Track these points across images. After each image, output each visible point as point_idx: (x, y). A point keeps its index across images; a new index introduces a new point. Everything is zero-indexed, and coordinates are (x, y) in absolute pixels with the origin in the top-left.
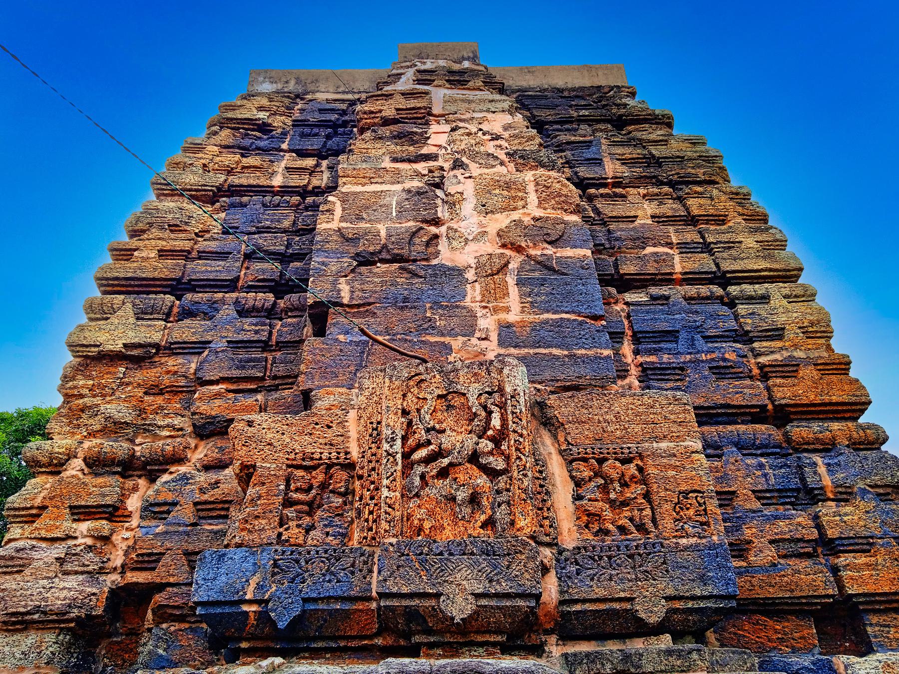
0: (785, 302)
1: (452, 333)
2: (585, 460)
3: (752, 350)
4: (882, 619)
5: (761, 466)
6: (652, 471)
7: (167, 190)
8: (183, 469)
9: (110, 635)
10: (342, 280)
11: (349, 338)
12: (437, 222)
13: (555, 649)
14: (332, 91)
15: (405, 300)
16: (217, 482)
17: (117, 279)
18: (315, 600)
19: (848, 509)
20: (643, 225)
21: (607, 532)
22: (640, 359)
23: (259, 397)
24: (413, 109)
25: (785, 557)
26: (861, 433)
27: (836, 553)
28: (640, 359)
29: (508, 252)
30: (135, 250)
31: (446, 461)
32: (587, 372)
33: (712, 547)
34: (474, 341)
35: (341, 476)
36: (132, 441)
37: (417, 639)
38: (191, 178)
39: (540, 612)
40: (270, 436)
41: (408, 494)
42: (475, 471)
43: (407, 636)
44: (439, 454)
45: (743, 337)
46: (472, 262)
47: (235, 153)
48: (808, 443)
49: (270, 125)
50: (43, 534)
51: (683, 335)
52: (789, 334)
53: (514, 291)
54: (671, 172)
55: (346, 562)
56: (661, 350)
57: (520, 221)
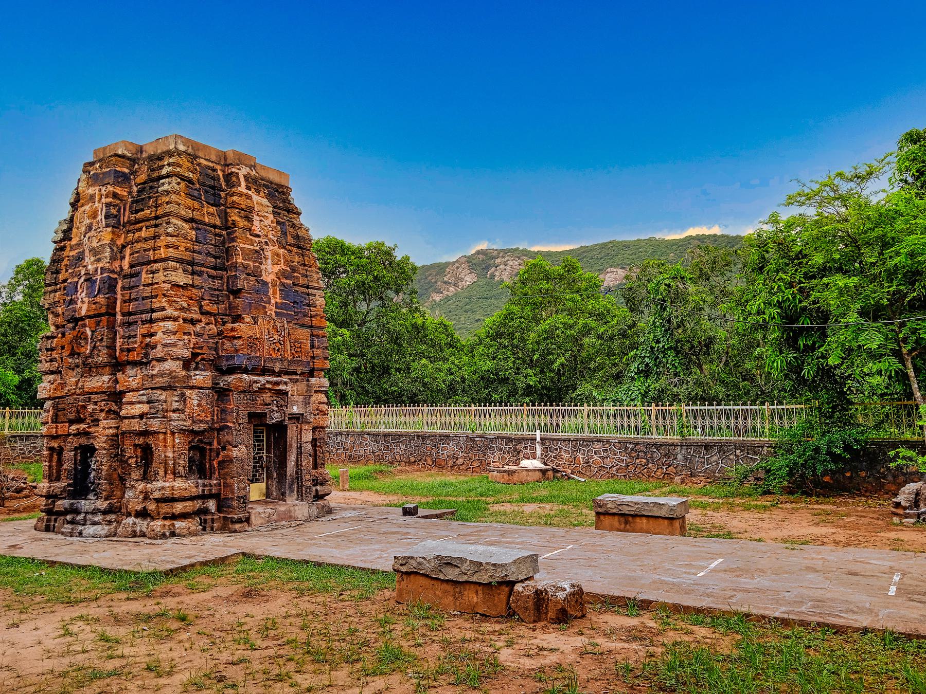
45: (309, 305)
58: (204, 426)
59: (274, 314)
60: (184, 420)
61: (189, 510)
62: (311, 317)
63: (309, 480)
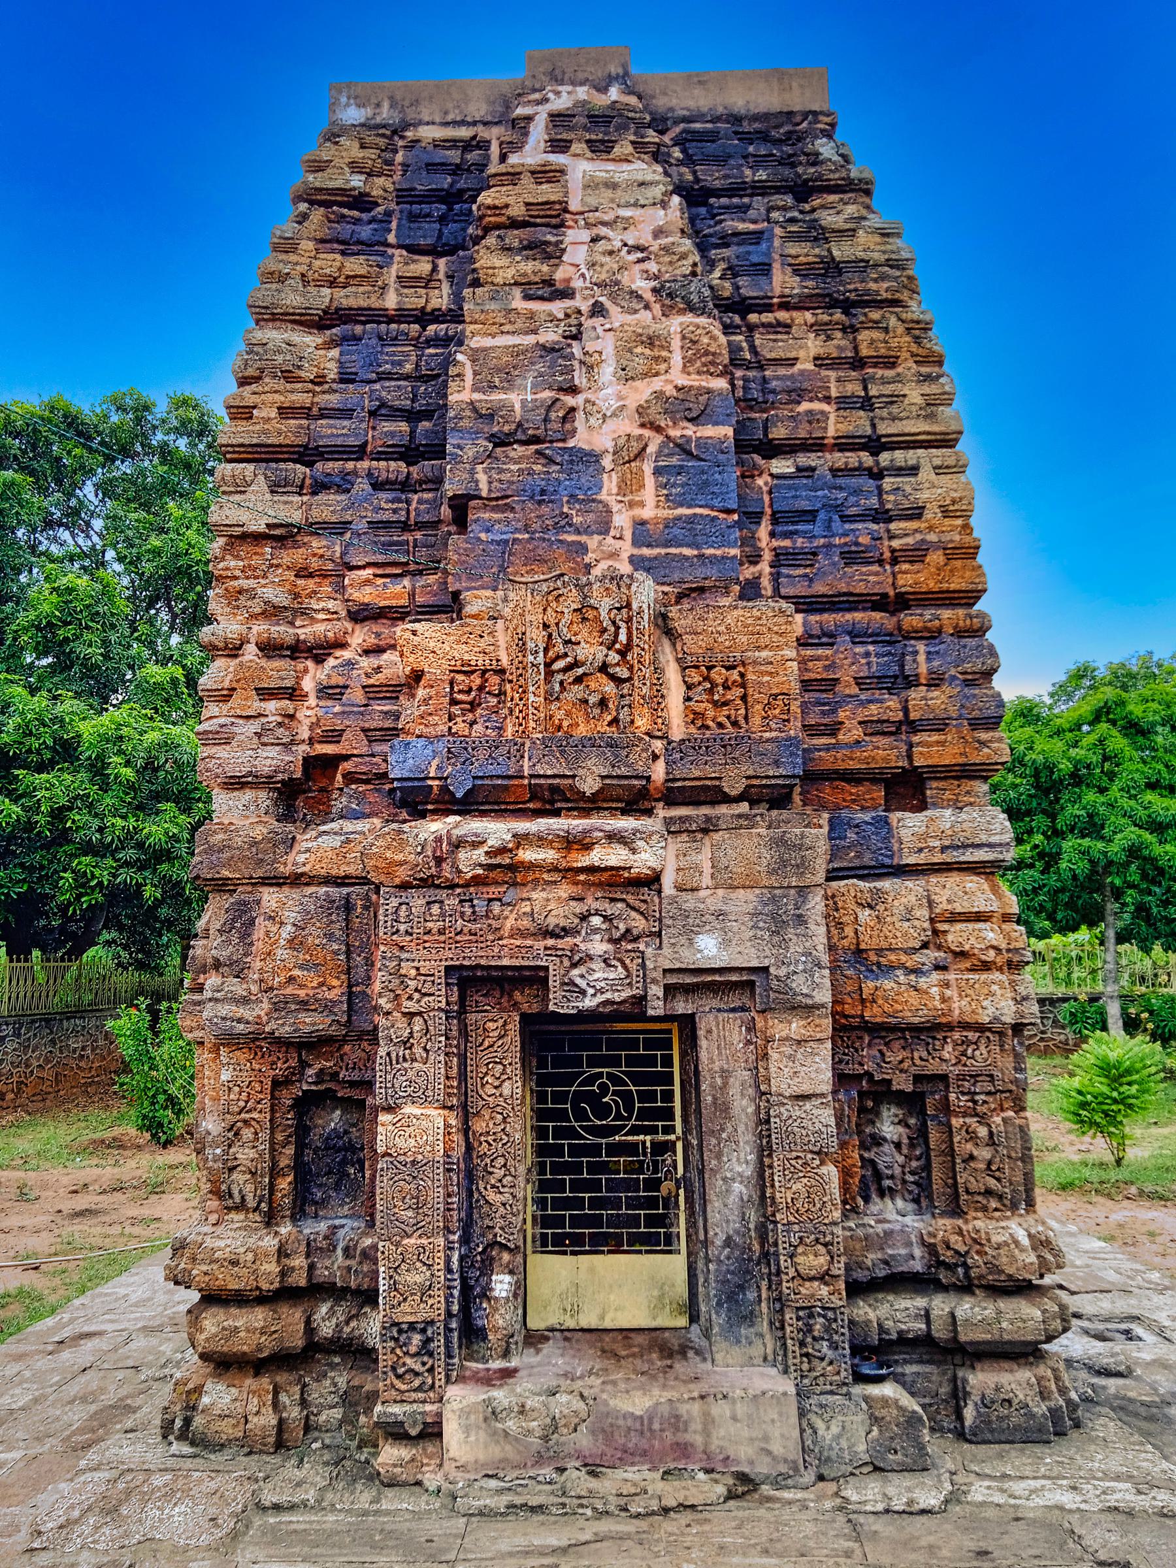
0: (933, 476)
1: (587, 531)
2: (696, 667)
3: (888, 531)
4: (941, 784)
5: (867, 654)
6: (750, 677)
7: (268, 316)
8: (347, 654)
9: (305, 792)
10: (479, 468)
11: (491, 537)
12: (573, 390)
13: (662, 812)
14: (438, 120)
15: (543, 492)
16: (379, 667)
17: (242, 445)
18: (482, 778)
19: (936, 693)
20: (802, 372)
21: (708, 728)
22: (775, 543)
23: (406, 582)
24: (546, 203)
25: (871, 734)
26: (968, 622)
27: (915, 731)
28: (775, 543)
29: (647, 433)
30: (254, 407)
31: (580, 671)
32: (713, 572)
33: (789, 739)
34: (609, 540)
35: (494, 680)
36: (292, 624)
37: (559, 805)
38: (292, 299)
39: (651, 787)
40: (432, 644)
41: (550, 697)
42: (604, 679)
43: (552, 802)
44: (576, 664)
46: (610, 446)
47: (333, 251)
48: (916, 632)
49: (368, 195)
50: (239, 712)
51: (822, 515)
52: (928, 515)
53: (650, 481)
54: (852, 285)
55: (503, 750)
56: (796, 532)
57: (662, 393)
58: (311, 1022)
59: (625, 568)
60: (245, 1001)
61: (244, 1344)
62: (894, 561)
63: (824, 1277)
